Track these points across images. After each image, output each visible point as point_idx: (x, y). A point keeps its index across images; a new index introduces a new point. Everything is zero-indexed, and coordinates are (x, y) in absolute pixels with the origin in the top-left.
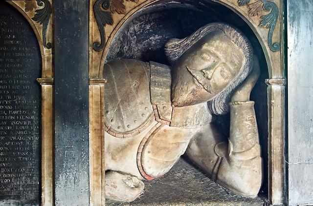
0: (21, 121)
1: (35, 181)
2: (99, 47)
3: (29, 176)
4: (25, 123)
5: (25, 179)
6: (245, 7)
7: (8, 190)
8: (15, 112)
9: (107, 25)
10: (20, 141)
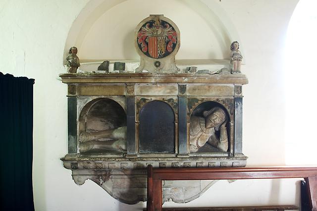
2: (188, 114)
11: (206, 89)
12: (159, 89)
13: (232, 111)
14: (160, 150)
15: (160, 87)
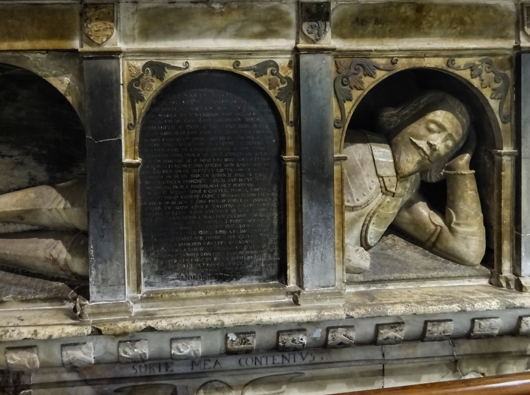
0: (262, 198)
1: (276, 257)
3: (270, 253)
4: (266, 200)
5: (266, 255)
6: (478, 78)
7: (251, 266)
8: (255, 190)
9: (347, 102)
10: (261, 218)
11: (405, 20)
12: (219, 21)
13: (507, 105)
14: (226, 273)
15: (221, 14)
